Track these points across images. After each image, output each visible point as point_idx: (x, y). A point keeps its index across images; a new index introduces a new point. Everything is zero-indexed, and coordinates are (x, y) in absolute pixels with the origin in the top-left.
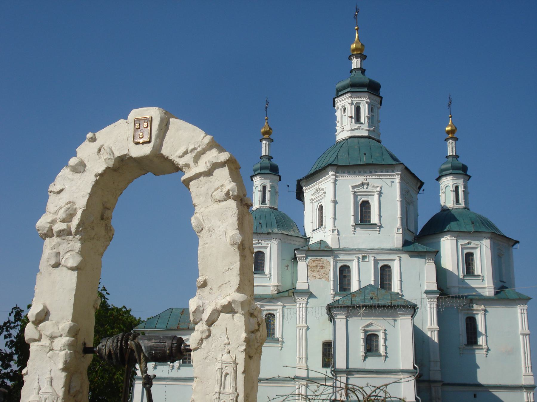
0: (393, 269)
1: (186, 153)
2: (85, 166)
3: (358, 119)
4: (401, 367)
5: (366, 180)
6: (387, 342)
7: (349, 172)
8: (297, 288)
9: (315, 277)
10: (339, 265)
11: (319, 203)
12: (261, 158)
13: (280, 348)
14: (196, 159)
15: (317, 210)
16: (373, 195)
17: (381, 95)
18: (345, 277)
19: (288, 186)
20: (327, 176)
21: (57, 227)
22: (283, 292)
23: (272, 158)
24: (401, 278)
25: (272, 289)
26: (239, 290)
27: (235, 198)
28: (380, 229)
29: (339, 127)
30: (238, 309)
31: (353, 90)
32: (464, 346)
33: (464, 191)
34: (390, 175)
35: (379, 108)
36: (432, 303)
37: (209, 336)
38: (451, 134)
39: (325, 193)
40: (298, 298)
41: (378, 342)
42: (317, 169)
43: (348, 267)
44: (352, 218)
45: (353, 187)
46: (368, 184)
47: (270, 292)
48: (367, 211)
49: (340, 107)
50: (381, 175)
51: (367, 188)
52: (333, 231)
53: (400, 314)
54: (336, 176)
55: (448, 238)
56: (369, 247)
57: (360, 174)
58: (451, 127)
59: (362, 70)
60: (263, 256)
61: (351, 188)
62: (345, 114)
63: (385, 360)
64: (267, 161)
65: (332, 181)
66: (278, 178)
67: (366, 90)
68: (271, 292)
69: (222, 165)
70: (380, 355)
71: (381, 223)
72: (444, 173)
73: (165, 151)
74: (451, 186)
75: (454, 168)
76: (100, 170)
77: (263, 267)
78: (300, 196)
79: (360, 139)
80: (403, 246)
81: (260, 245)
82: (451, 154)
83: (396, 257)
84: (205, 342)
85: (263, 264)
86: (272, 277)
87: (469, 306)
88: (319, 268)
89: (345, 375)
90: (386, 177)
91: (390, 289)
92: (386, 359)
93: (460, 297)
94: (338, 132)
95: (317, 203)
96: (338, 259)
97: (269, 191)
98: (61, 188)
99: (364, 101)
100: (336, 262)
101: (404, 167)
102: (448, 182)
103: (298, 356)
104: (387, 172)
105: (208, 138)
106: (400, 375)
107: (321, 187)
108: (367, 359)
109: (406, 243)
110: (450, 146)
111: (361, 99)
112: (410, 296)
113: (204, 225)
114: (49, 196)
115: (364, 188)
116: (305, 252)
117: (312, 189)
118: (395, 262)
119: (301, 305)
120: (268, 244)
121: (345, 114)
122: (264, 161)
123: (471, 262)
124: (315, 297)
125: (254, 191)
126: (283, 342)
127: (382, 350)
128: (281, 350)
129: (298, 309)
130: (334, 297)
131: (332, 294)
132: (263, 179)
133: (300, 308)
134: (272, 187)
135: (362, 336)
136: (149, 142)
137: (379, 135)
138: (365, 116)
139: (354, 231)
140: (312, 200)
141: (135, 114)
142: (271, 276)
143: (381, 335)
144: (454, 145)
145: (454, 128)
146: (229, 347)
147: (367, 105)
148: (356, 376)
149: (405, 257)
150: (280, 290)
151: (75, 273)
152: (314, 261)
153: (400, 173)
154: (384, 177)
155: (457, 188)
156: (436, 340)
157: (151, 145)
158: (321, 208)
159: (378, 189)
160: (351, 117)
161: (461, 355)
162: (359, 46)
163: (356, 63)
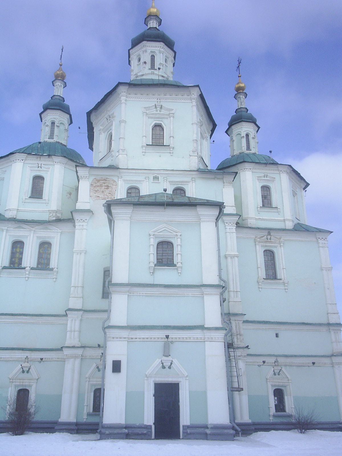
5: (159, 102)
9: (98, 197)
11: (108, 132)
15: (106, 139)
32: (263, 280)
36: (231, 227)
40: (78, 220)
55: (243, 170)
81: (40, 169)
87: (267, 239)
88: (103, 188)
101: (200, 93)
115: (157, 111)
121: (139, 63)
150: (59, 217)
158: (111, 136)
161: (260, 289)
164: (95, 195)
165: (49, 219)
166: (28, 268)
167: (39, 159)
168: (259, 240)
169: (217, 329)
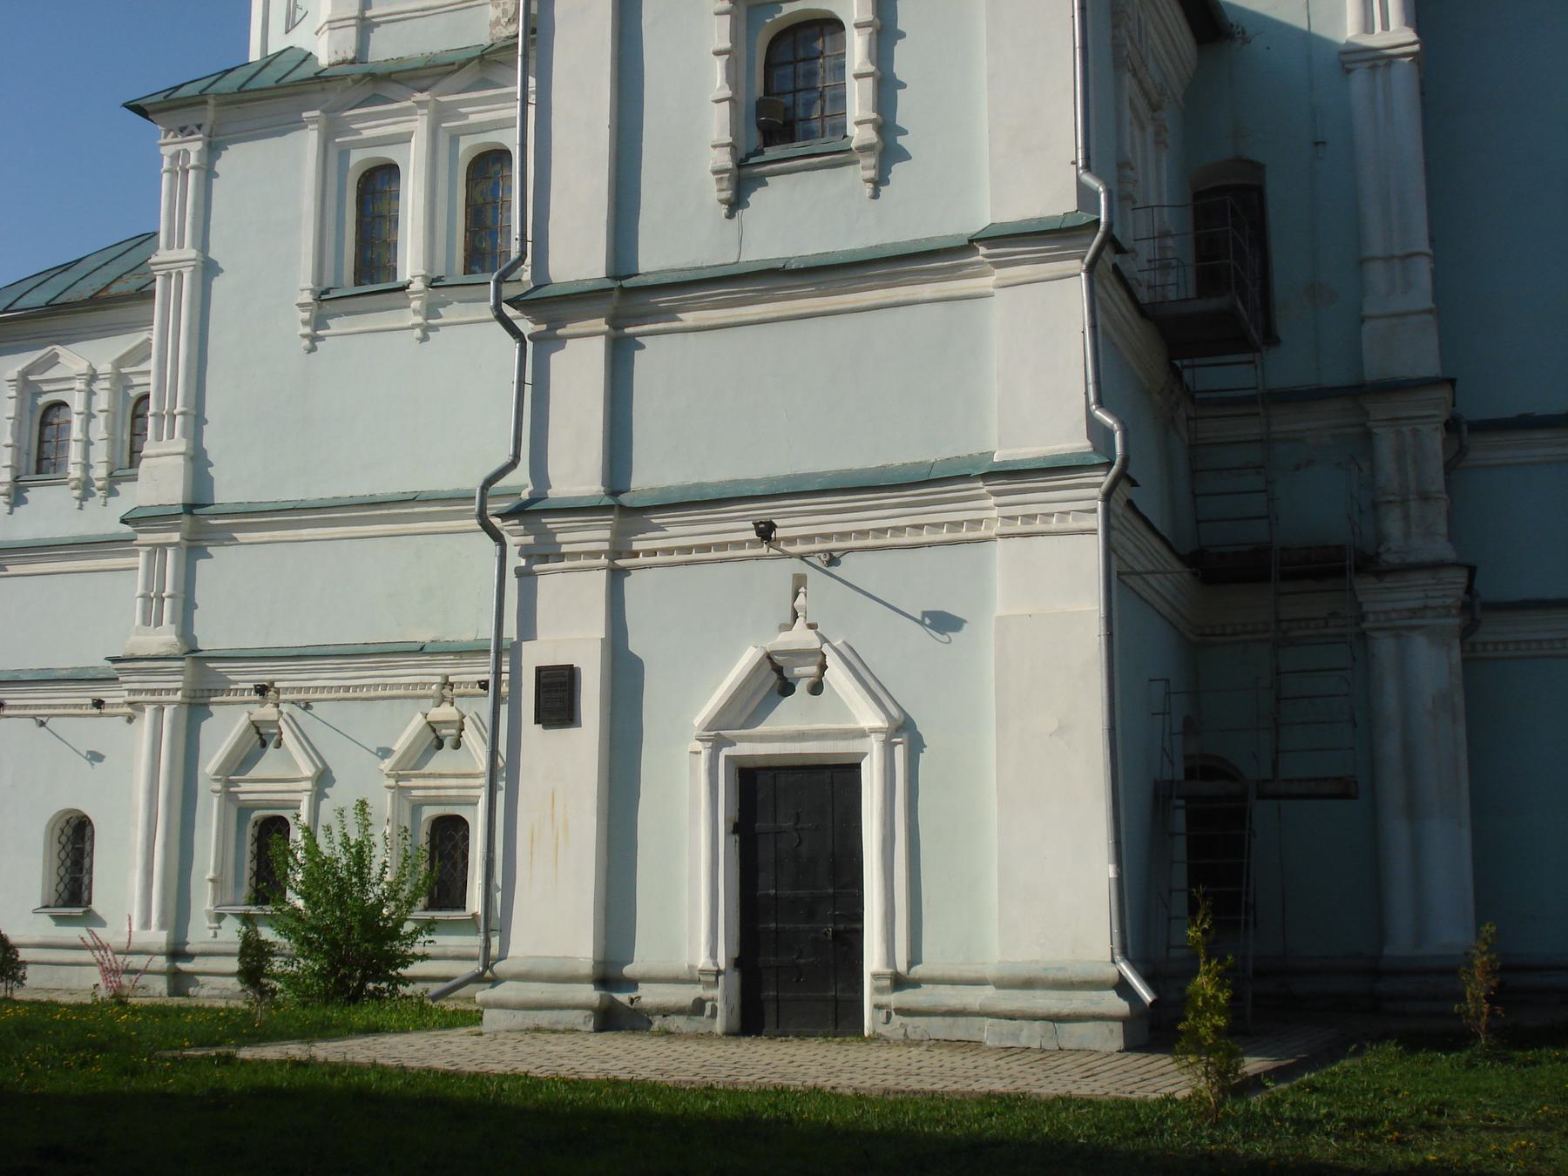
4: (984, 215)
6: (901, 51)
63: (879, 182)
68: (488, 30)
70: (842, 157)
108: (757, 198)
165: (491, 33)
166: (418, 285)
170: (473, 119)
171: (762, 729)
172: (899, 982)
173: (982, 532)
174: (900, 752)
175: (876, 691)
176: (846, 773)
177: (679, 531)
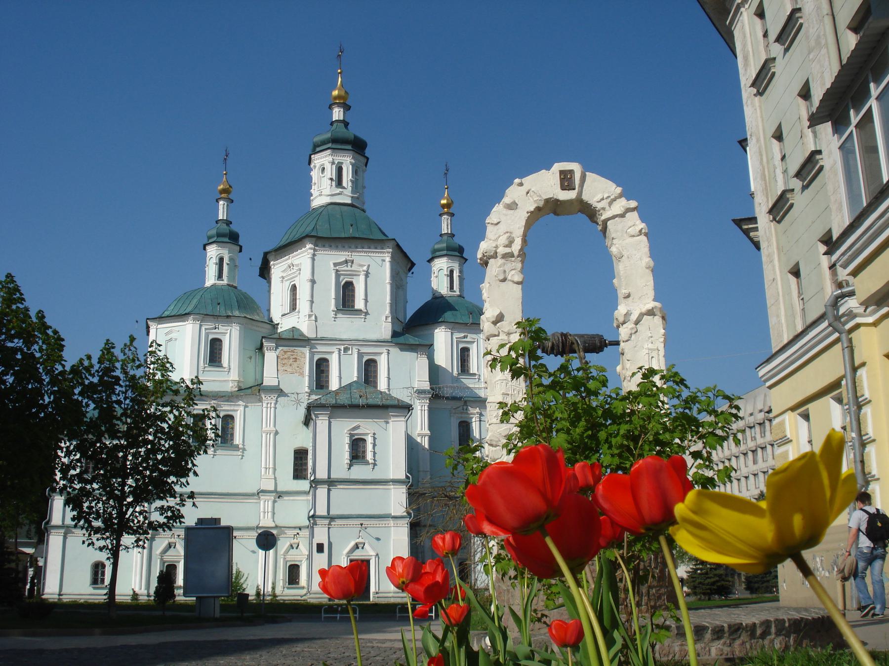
0: (380, 364)
1: (603, 199)
2: (517, 205)
3: (339, 183)
6: (376, 447)
7: (331, 246)
8: (264, 384)
10: (316, 357)
12: (217, 222)
13: (240, 457)
14: (610, 204)
16: (359, 275)
17: (366, 155)
18: (322, 372)
19: (251, 259)
20: (303, 249)
21: (501, 250)
22: (245, 389)
23: (231, 223)
24: (389, 374)
25: (231, 384)
26: (654, 300)
27: (646, 235)
28: (365, 316)
29: (316, 190)
30: (658, 312)
31: (334, 146)
33: (459, 276)
34: (379, 252)
35: (364, 171)
36: (422, 404)
37: (636, 332)
38: (447, 208)
39: (300, 270)
41: (365, 447)
42: (288, 241)
43: (326, 361)
44: (333, 302)
45: (335, 265)
46: (352, 262)
47: (229, 390)
48: (351, 294)
49: (318, 166)
50: (369, 252)
51: (351, 267)
52: (310, 316)
53: (392, 415)
54: (315, 250)
56: (352, 338)
57: (343, 248)
58: (447, 200)
59: (345, 123)
60: (221, 345)
61: (332, 266)
62: (323, 175)
63: (373, 469)
64: (224, 226)
65: (310, 256)
66: (238, 248)
67: (349, 147)
69: (633, 210)
70: (367, 463)
71: (366, 309)
72: (438, 254)
73: (585, 197)
74: (445, 269)
75: (449, 248)
76: (532, 209)
77: (220, 358)
78: (265, 271)
79: (342, 207)
80: (392, 337)
81: (217, 331)
82: (446, 232)
83: (384, 350)
84: (633, 336)
85: (220, 354)
86: (232, 371)
87: (463, 409)
88: (291, 360)
89: (327, 486)
90: (374, 255)
91: (376, 386)
92: (374, 466)
93: (454, 398)
94: (314, 196)
95: (289, 282)
96: (314, 350)
97: (228, 264)
98: (498, 221)
99: (347, 161)
100: (312, 354)
101: (396, 244)
102: (442, 265)
103: (263, 466)
104: (376, 248)
105: (619, 190)
106: (390, 485)
107: (295, 262)
109: (395, 334)
110: (446, 223)
111: (344, 159)
112: (404, 396)
113: (624, 253)
114: (486, 227)
115: (347, 267)
116: (275, 340)
117: (283, 264)
118: (383, 354)
119: (269, 405)
120: (227, 330)
121: (323, 175)
122: (221, 227)
123: (466, 358)
124: (286, 395)
125: (207, 263)
126: (244, 449)
127: (369, 456)
128: (242, 458)
129: (264, 410)
130: (309, 396)
131: (307, 392)
132: (220, 248)
133: (267, 408)
134: (231, 259)
135: (347, 440)
136: (574, 189)
137: (364, 203)
138: (349, 179)
139: (335, 318)
140: (283, 277)
141: (558, 167)
142: (230, 369)
143: (369, 440)
144: (449, 221)
145: (450, 202)
146: (652, 339)
147: (351, 166)
148: (339, 487)
149: (395, 351)
151: (520, 286)
152: (285, 352)
153: (391, 250)
154: (372, 255)
155: (452, 272)
156: (427, 446)
157: (576, 191)
158: (294, 288)
159: (365, 268)
160: (331, 179)
162: (343, 93)
163: (337, 114)
164: (283, 368)
167: (216, 319)
168: (454, 411)
169: (402, 517)
170: (224, 408)
171: (353, 554)
172: (377, 593)
173: (389, 525)
174: (377, 559)
175: (373, 549)
176: (368, 562)
177: (339, 522)
